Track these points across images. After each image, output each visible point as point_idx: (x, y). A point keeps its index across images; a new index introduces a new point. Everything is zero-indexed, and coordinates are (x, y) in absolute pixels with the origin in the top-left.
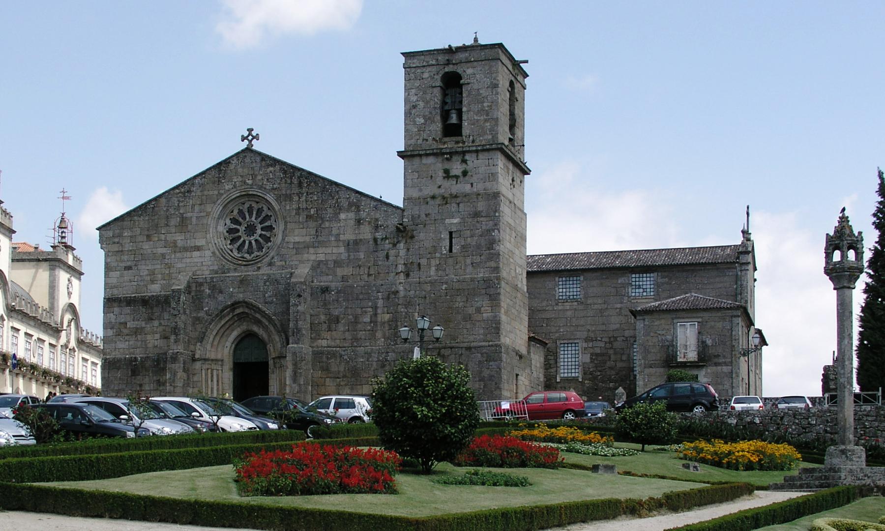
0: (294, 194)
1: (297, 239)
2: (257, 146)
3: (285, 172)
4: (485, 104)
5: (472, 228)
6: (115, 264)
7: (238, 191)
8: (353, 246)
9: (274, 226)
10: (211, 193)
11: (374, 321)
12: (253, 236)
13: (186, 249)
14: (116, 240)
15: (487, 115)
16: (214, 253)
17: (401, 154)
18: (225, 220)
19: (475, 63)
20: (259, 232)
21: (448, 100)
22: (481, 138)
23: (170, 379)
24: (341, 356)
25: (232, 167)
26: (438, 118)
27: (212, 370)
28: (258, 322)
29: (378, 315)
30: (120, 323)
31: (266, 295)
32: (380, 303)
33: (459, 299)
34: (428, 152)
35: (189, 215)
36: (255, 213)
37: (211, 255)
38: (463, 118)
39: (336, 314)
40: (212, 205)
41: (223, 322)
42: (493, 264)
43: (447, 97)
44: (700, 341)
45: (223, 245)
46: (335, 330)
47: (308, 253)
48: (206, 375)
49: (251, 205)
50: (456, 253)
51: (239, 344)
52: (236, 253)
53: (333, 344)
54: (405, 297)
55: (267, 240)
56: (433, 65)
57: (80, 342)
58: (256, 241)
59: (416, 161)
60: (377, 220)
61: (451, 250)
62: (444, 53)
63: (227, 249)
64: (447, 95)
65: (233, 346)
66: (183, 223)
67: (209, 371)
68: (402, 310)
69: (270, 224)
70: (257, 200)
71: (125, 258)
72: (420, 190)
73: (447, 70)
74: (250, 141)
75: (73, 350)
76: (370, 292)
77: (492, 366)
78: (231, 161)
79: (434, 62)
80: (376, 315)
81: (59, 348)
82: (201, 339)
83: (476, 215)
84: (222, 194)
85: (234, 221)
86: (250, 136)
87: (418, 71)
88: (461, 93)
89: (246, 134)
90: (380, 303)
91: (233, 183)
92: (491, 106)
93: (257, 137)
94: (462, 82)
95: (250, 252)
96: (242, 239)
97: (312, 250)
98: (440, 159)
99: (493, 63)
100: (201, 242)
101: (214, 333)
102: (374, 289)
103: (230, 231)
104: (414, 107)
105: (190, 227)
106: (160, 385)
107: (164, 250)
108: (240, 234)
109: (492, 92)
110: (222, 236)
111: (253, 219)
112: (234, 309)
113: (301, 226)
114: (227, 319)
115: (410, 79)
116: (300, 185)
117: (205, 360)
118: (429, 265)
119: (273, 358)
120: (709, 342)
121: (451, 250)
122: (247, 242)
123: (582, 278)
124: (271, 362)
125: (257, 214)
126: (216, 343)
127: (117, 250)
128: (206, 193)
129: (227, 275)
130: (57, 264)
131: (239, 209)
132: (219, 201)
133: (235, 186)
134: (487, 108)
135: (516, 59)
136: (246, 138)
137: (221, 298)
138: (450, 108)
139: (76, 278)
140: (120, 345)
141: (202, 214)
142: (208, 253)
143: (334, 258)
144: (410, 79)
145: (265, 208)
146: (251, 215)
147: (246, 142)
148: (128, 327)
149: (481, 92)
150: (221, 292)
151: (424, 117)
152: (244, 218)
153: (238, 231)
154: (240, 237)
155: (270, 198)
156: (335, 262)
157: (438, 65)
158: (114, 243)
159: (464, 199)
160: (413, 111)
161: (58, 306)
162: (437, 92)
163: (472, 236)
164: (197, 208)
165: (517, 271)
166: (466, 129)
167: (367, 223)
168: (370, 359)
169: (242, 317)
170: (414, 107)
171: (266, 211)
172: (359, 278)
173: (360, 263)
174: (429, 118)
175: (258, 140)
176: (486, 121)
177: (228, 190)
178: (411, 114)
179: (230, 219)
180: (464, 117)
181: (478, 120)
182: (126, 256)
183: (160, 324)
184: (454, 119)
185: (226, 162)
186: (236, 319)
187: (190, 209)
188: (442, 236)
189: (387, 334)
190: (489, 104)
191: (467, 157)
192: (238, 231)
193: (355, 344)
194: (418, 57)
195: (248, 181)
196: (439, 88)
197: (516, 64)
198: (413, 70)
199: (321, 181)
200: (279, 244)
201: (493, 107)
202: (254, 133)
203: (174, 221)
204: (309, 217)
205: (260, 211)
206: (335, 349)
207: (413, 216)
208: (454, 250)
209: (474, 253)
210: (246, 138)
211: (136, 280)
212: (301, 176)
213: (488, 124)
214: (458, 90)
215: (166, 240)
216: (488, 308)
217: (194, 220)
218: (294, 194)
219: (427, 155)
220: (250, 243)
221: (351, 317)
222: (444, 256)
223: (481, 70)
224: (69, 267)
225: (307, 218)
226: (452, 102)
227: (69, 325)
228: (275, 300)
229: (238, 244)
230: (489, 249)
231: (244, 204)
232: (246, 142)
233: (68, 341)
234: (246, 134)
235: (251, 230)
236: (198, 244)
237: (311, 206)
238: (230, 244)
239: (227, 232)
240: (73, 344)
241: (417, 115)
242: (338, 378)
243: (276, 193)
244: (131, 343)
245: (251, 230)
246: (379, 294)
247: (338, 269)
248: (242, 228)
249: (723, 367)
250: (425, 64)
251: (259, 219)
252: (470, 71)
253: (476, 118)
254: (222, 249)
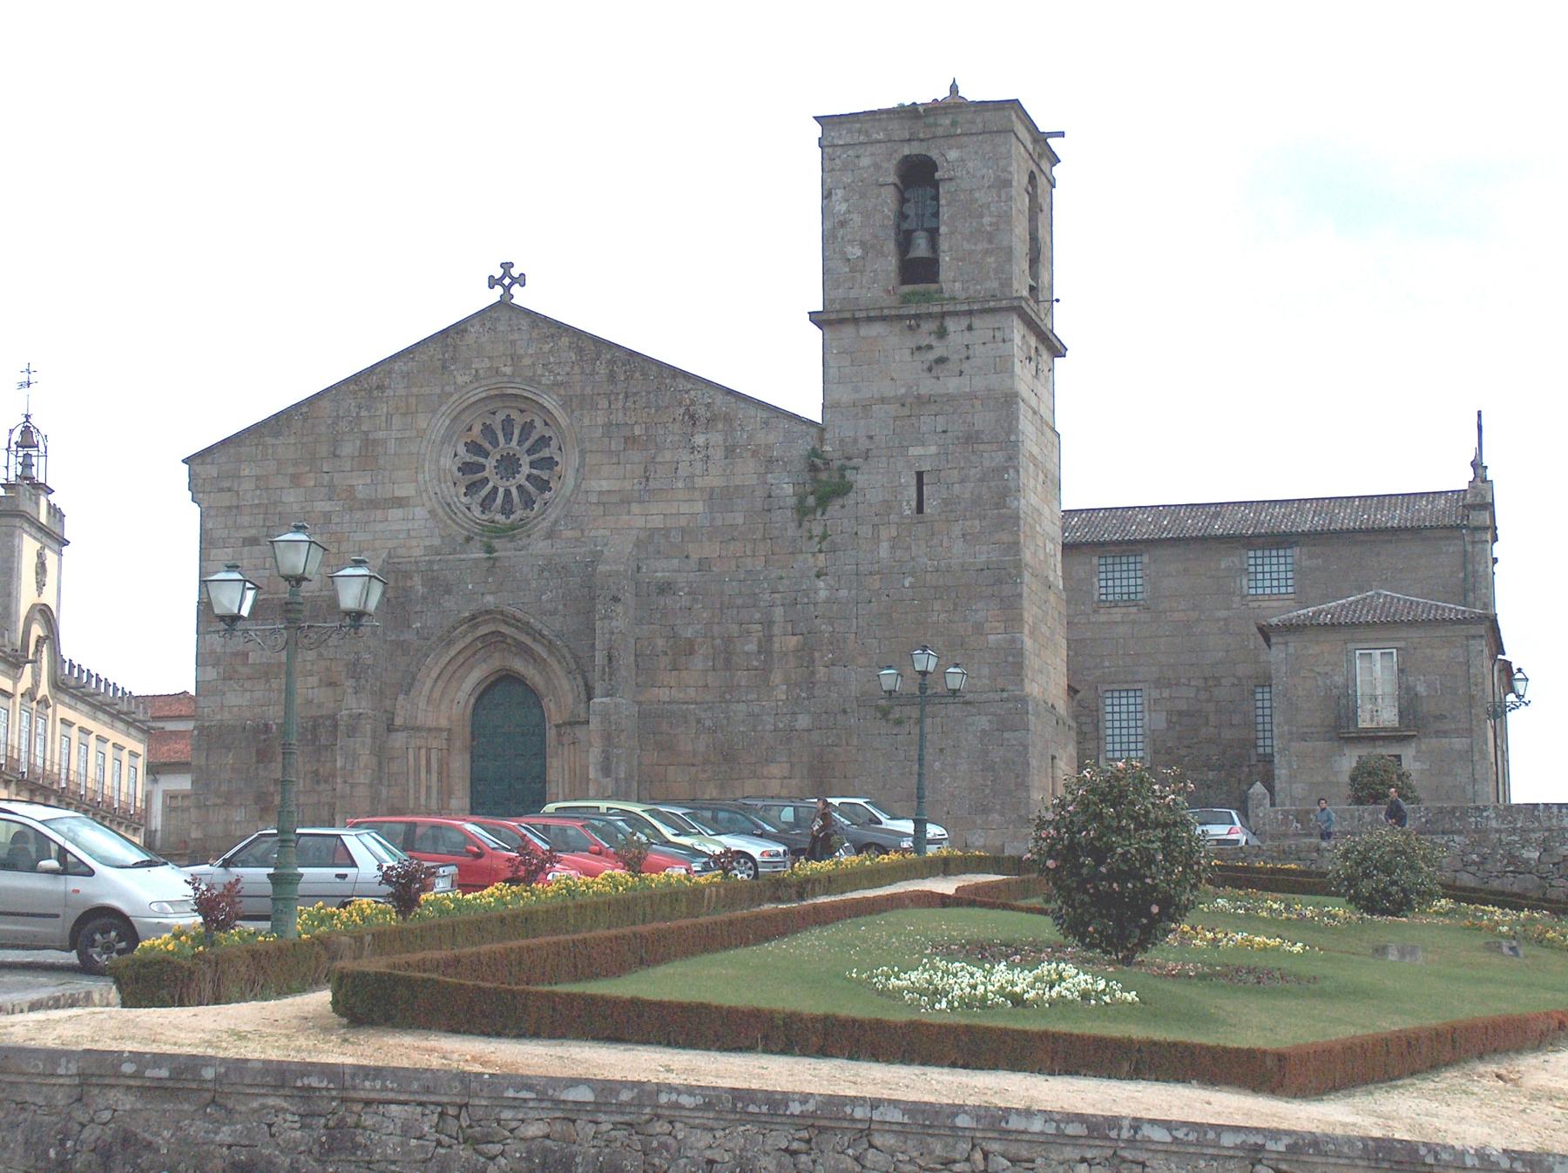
0: (599, 394)
1: (605, 485)
2: (520, 297)
3: (580, 351)
4: (986, 220)
5: (962, 465)
6: (224, 533)
7: (482, 389)
8: (721, 498)
10: (426, 390)
11: (765, 647)
12: (514, 478)
13: (373, 504)
14: (226, 484)
15: (990, 242)
16: (432, 512)
17: (815, 317)
18: (455, 446)
19: (965, 139)
20: (526, 470)
21: (910, 209)
22: (979, 287)
23: (343, 768)
24: (698, 721)
25: (470, 339)
26: (891, 246)
27: (429, 750)
28: (525, 651)
29: (775, 639)
30: (235, 654)
31: (543, 597)
32: (779, 612)
33: (937, 606)
34: (872, 314)
35: (381, 435)
36: (517, 432)
37: (429, 516)
38: (942, 248)
39: (689, 636)
40: (430, 415)
41: (452, 653)
42: (1006, 537)
43: (907, 205)
44: (1403, 686)
45: (451, 497)
46: (686, 669)
47: (629, 513)
48: (417, 759)
49: (509, 416)
50: (932, 515)
51: (485, 694)
52: (477, 511)
53: (681, 695)
54: (828, 600)
55: (544, 486)
56: (879, 142)
57: (58, 685)
58: (520, 487)
59: (848, 330)
60: (769, 447)
61: (920, 509)
62: (902, 118)
63: (458, 505)
64: (908, 201)
65: (472, 701)
66: (369, 455)
67: (423, 751)
68: (824, 627)
69: (548, 455)
70: (523, 406)
71: (245, 520)
72: (856, 390)
73: (907, 152)
74: (507, 289)
75: (44, 702)
76: (757, 591)
77: (1008, 740)
78: (469, 328)
79: (881, 136)
80: (770, 638)
81: (18, 699)
82: (407, 685)
83: (971, 439)
84: (451, 395)
85: (474, 447)
86: (508, 277)
87: (850, 152)
88: (936, 198)
89: (498, 273)
90: (779, 612)
91: (474, 372)
92: (997, 223)
93: (521, 280)
94: (938, 175)
95: (507, 510)
96: (491, 484)
97: (635, 508)
98: (897, 327)
99: (999, 139)
100: (406, 490)
101: (434, 675)
102: (766, 585)
103: (466, 468)
104: (843, 224)
105: (381, 462)
106: (318, 782)
107: (327, 506)
108: (486, 474)
109: (1000, 197)
110: (449, 477)
111: (514, 443)
112: (476, 626)
113: (615, 460)
114: (460, 645)
115: (833, 170)
116: (612, 377)
117: (417, 729)
118: (876, 539)
119: (557, 726)
120: (1421, 689)
121: (920, 509)
122: (501, 490)
123: (1146, 559)
124: (551, 734)
125: (520, 436)
126: (436, 695)
127: (228, 504)
128: (415, 390)
129: (462, 556)
130: (17, 522)
131: (484, 424)
132: (444, 408)
133: (477, 377)
134: (989, 228)
135: (1041, 130)
136: (499, 281)
137: (449, 603)
138: (914, 226)
139: (54, 551)
140: (233, 699)
141: (408, 434)
142: (420, 512)
143: (683, 522)
144: (833, 170)
145: (538, 423)
146: (508, 436)
147: (499, 290)
148: (250, 661)
149: (977, 195)
150: (448, 592)
151: (863, 244)
152: (495, 443)
153: (483, 467)
154: (486, 480)
155: (549, 402)
156: (683, 530)
157: (889, 141)
158: (221, 490)
159: (947, 408)
160: (841, 232)
161: (17, 612)
162: (889, 197)
163: (962, 481)
164: (397, 421)
165: (1048, 550)
166: (947, 270)
167: (750, 453)
168: (760, 728)
169: (494, 641)
170: (843, 224)
171: (540, 429)
172: (733, 563)
173: (736, 534)
174: (873, 246)
175: (523, 285)
176: (987, 252)
177: (463, 387)
178: (835, 237)
179: (466, 444)
180: (944, 245)
181: (971, 252)
182: (247, 518)
183: (320, 655)
184: (921, 249)
185: (459, 329)
186: (480, 646)
187: (384, 424)
188: (903, 480)
189: (793, 676)
190: (994, 220)
191: (951, 325)
192: (483, 467)
193: (728, 697)
194: (849, 126)
195: (504, 369)
196: (892, 187)
197: (1040, 138)
198: (839, 151)
199: (654, 368)
200: (568, 494)
201: (1002, 226)
202: (515, 272)
203: (348, 448)
204: (631, 441)
205: (528, 428)
206: (685, 706)
207: (842, 441)
208: (927, 510)
209: (968, 514)
210: (499, 281)
211: (267, 565)
212: (612, 362)
213: (993, 259)
214: (930, 191)
215: (331, 486)
216: (998, 624)
217: (392, 445)
218: (599, 394)
219: (869, 319)
220: (508, 493)
221: (718, 641)
222: (906, 521)
223: (976, 153)
224: (41, 528)
225: (625, 443)
226: (916, 215)
227: (38, 650)
228: (561, 607)
229: (484, 493)
230: (997, 506)
231: (494, 413)
232: (499, 290)
233: (36, 684)
234: (498, 273)
235: (509, 465)
236: (398, 493)
237: (634, 418)
238: (465, 494)
239: (459, 469)
240: (44, 690)
241: (849, 241)
242: (694, 765)
243: (562, 392)
244: (257, 694)
245: (509, 465)
246: (776, 595)
247: (690, 545)
248: (490, 463)
249: (1454, 740)
250: (862, 138)
251: (527, 445)
252: (953, 155)
253: (966, 246)
254: (449, 505)
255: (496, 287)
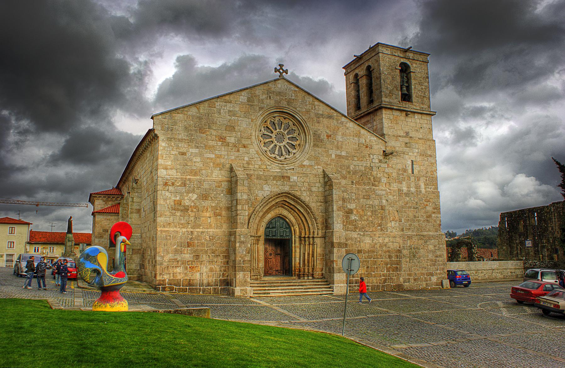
9: (297, 138)
73: (402, 60)
74: (281, 74)
121: (413, 173)
169: (284, 204)
202: (278, 68)
210: (279, 71)
255: (285, 70)
